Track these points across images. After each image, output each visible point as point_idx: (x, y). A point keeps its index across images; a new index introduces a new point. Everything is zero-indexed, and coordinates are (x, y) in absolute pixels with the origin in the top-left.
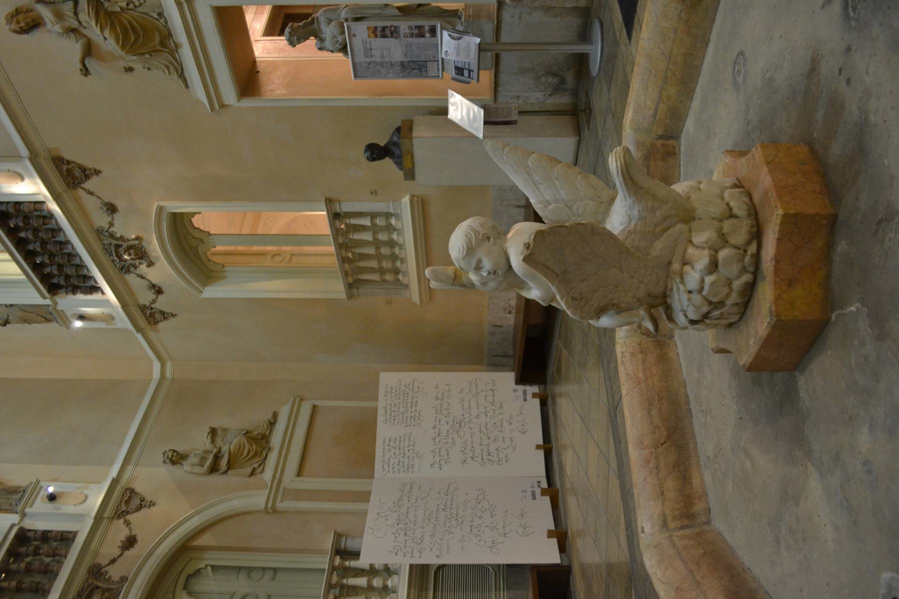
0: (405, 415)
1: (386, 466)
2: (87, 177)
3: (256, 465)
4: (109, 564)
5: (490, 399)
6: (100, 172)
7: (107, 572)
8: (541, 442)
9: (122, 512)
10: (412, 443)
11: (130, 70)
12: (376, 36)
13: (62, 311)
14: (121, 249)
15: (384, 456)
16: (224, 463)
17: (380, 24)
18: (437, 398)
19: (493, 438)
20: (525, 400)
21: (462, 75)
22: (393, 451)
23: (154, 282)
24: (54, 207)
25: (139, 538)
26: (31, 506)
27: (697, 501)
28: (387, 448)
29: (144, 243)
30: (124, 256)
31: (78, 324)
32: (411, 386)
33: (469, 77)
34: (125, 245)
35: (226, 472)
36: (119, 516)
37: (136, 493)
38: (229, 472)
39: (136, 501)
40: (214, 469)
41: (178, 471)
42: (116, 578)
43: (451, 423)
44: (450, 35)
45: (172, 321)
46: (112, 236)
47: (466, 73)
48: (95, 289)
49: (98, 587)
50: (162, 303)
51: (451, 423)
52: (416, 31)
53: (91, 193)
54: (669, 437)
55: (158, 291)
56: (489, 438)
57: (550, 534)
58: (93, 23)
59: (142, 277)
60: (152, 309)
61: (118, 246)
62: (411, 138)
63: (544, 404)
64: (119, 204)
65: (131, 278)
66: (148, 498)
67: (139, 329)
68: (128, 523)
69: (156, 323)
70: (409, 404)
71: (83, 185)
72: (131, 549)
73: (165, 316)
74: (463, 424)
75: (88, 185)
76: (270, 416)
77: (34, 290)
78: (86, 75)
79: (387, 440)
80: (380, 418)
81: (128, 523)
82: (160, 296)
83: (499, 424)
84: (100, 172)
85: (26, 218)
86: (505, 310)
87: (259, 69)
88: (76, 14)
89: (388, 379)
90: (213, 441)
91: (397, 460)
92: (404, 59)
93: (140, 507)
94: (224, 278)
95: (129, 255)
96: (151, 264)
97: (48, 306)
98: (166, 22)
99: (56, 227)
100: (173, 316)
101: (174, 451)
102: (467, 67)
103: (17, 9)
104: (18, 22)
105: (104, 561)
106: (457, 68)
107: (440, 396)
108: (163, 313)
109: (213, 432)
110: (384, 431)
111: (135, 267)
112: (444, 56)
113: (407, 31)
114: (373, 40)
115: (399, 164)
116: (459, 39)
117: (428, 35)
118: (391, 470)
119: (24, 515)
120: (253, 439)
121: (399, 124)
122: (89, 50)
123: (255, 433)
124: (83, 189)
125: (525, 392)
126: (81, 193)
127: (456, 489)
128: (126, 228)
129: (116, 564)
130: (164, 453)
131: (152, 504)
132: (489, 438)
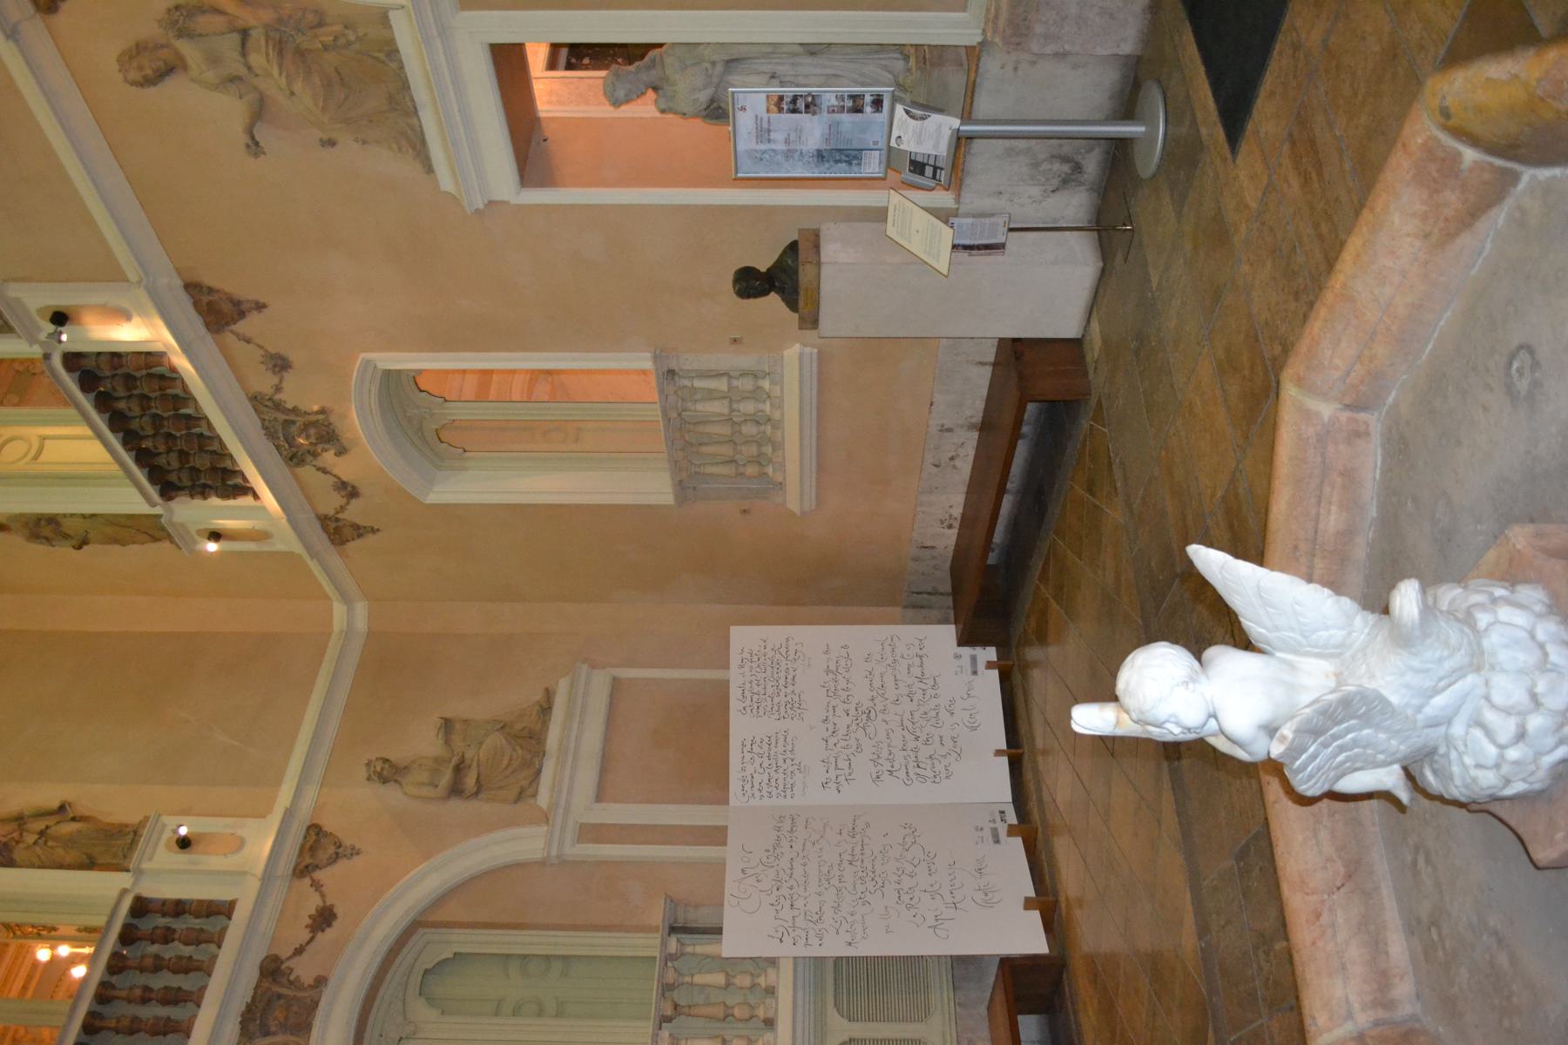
0: (776, 700)
1: (748, 787)
2: (242, 315)
3: (525, 783)
5: (916, 671)
6: (264, 306)
7: (292, 970)
8: (1002, 744)
10: (789, 748)
11: (332, 143)
12: (780, 110)
13: (182, 525)
14: (294, 429)
15: (743, 769)
16: (470, 781)
17: (789, 91)
18: (828, 671)
19: (923, 737)
20: (975, 673)
21: (922, 173)
22: (758, 761)
23: (345, 479)
24: (182, 363)
25: (338, 910)
26: (150, 859)
27: (1396, 980)
28: (748, 756)
29: (333, 419)
30: (300, 438)
31: (212, 547)
32: (783, 651)
33: (934, 177)
34: (300, 421)
35: (477, 793)
37: (326, 834)
38: (481, 796)
40: (456, 790)
41: (393, 795)
43: (852, 712)
44: (907, 112)
45: (370, 539)
46: (278, 406)
47: (929, 171)
48: (229, 483)
49: (279, 996)
50: (355, 512)
51: (852, 712)
52: (849, 103)
53: (248, 341)
54: (1349, 876)
55: (350, 491)
56: (917, 738)
57: (1029, 904)
58: (275, 72)
59: (324, 471)
60: (337, 520)
61: (288, 423)
62: (819, 264)
63: (1005, 678)
64: (294, 356)
65: (307, 472)
66: (347, 842)
67: (314, 555)
68: (317, 885)
69: (343, 542)
70: (782, 682)
71: (233, 327)
72: (328, 930)
73: (359, 531)
74: (873, 714)
75: (241, 326)
76: (539, 696)
77: (134, 491)
78: (256, 155)
79: (748, 743)
80: (735, 705)
81: (317, 885)
82: (353, 501)
83: (933, 713)
84: (264, 306)
85: (129, 379)
86: (942, 522)
87: (547, 134)
88: (244, 54)
89: (744, 638)
90: (447, 742)
91: (765, 777)
92: (823, 147)
93: (336, 857)
94: (464, 469)
95: (308, 437)
96: (341, 452)
97: (160, 516)
98: (402, 67)
99: (182, 394)
100: (374, 531)
101: (386, 760)
102: (931, 162)
103: (137, 46)
104: (141, 68)
105: (285, 952)
106: (913, 163)
107: (833, 667)
108: (356, 527)
109: (447, 725)
110: (742, 727)
111: (315, 455)
112: (893, 143)
113: (834, 102)
114: (775, 116)
115: (793, 305)
116: (923, 118)
117: (868, 109)
118: (757, 794)
120: (516, 737)
121: (795, 237)
122: (260, 111)
123: (518, 727)
124: (237, 335)
125: (974, 659)
126: (229, 338)
127: (868, 825)
128: (302, 394)
129: (305, 956)
130: (368, 765)
131: (354, 852)
132: (917, 738)
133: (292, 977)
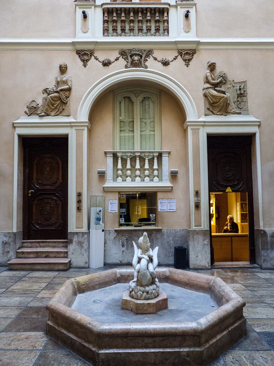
4: (154, 57)
9: (181, 53)
36: (179, 52)
39: (187, 57)
42: (147, 63)
49: (141, 57)
72: (162, 65)
119: (176, 7)
131: (187, 65)
133: (147, 59)
